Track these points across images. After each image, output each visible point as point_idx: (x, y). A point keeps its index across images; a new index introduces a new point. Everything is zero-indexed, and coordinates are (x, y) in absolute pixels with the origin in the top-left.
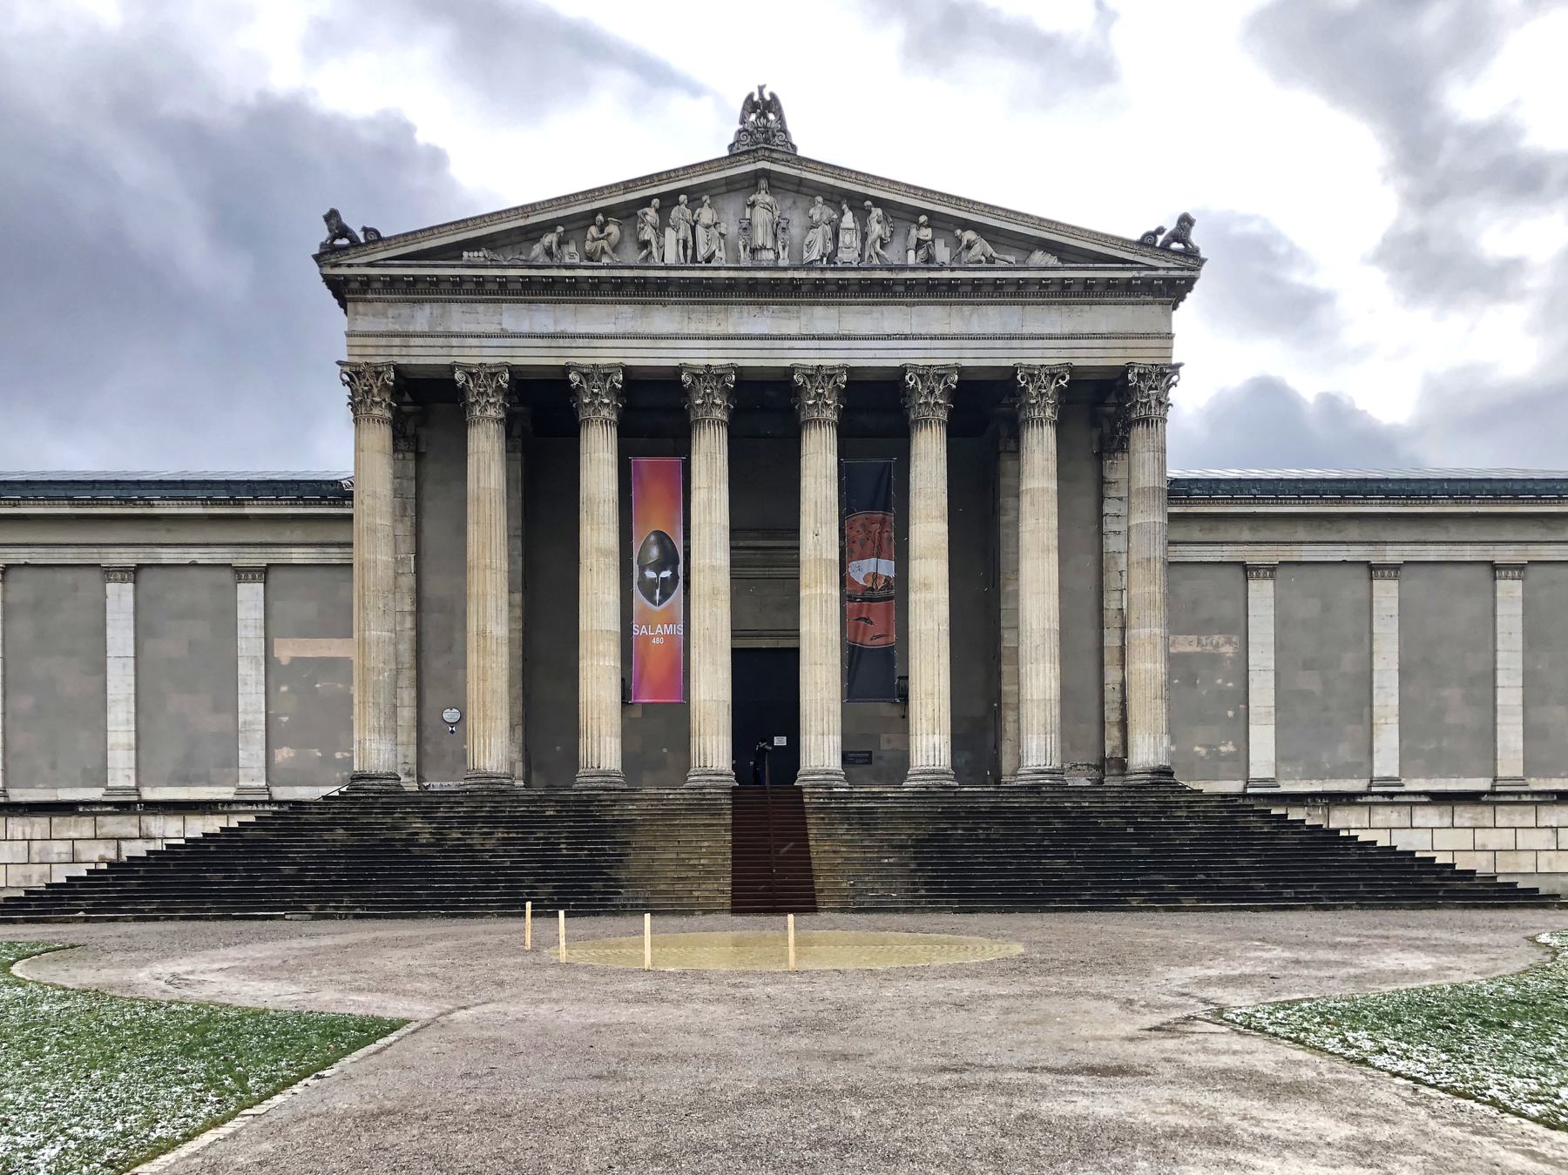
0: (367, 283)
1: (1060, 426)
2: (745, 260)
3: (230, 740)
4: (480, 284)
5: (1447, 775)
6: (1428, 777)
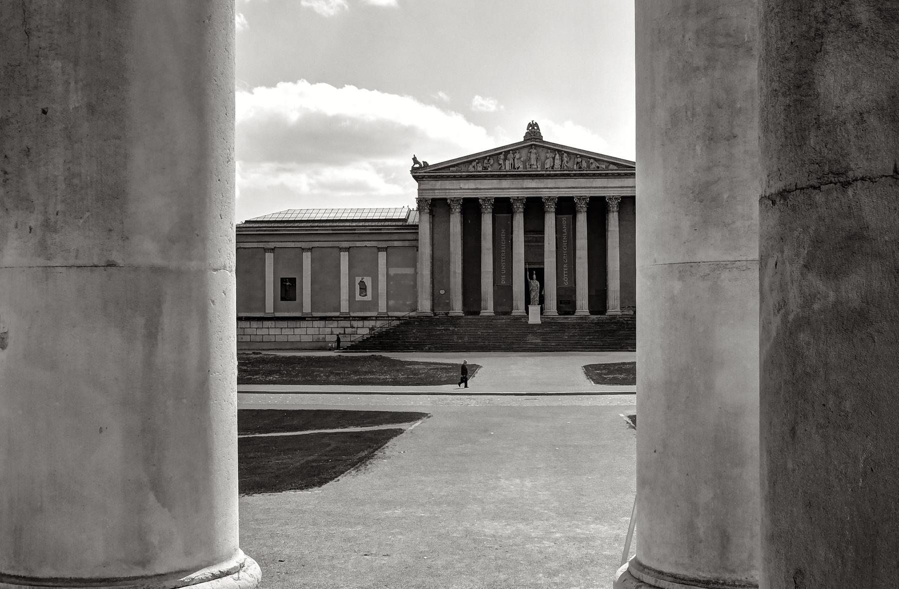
0: (423, 177)
1: (619, 212)
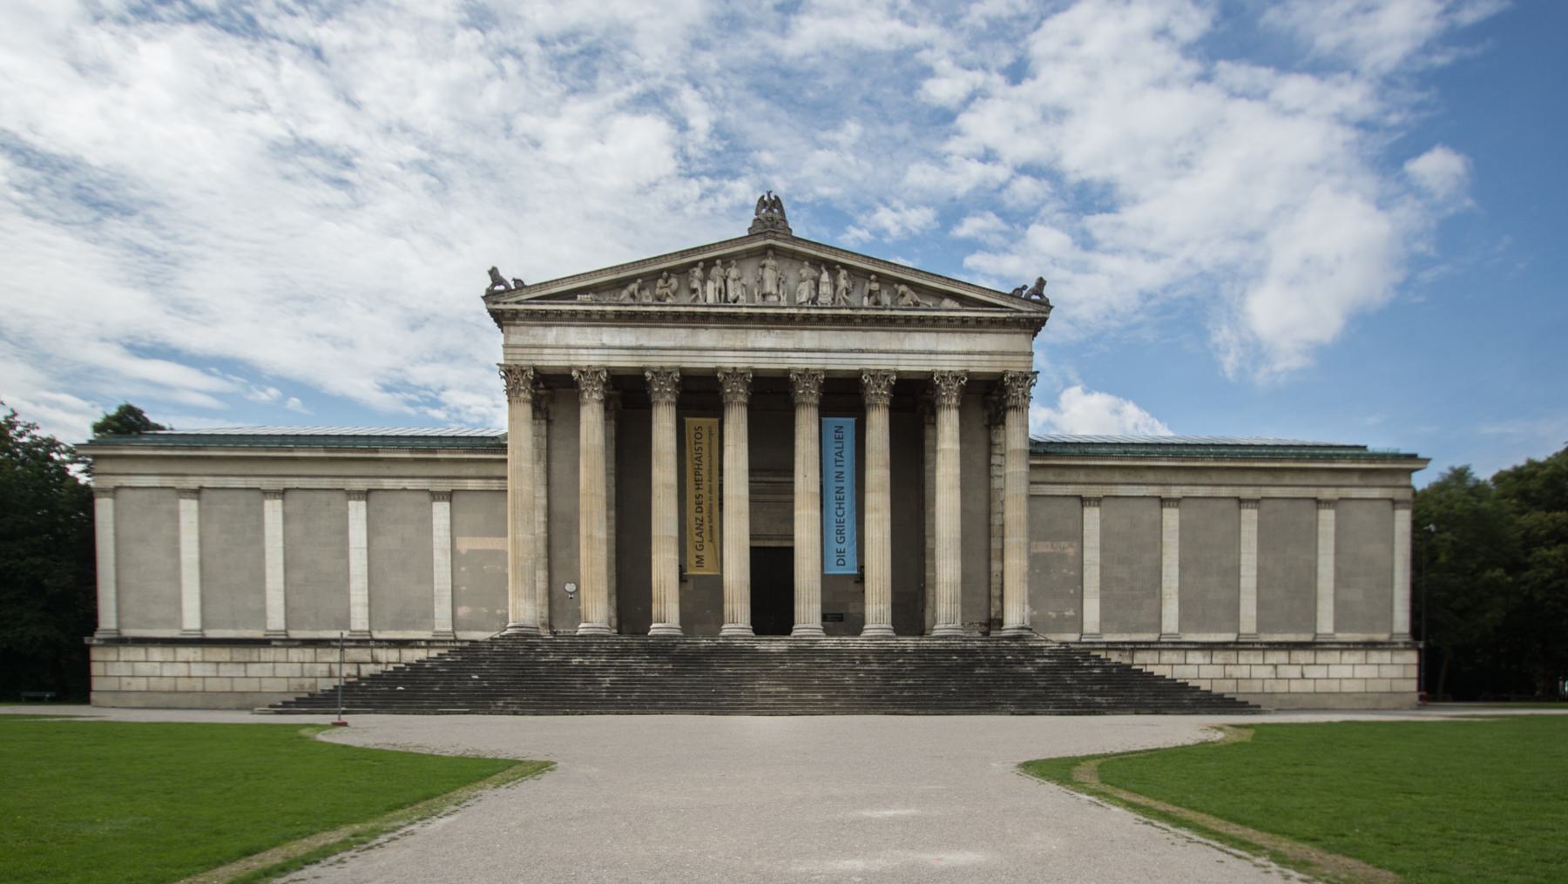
0: (515, 314)
1: (962, 410)
2: (758, 300)
3: (429, 600)
4: (588, 314)
5: (1209, 631)
6: (1197, 632)
